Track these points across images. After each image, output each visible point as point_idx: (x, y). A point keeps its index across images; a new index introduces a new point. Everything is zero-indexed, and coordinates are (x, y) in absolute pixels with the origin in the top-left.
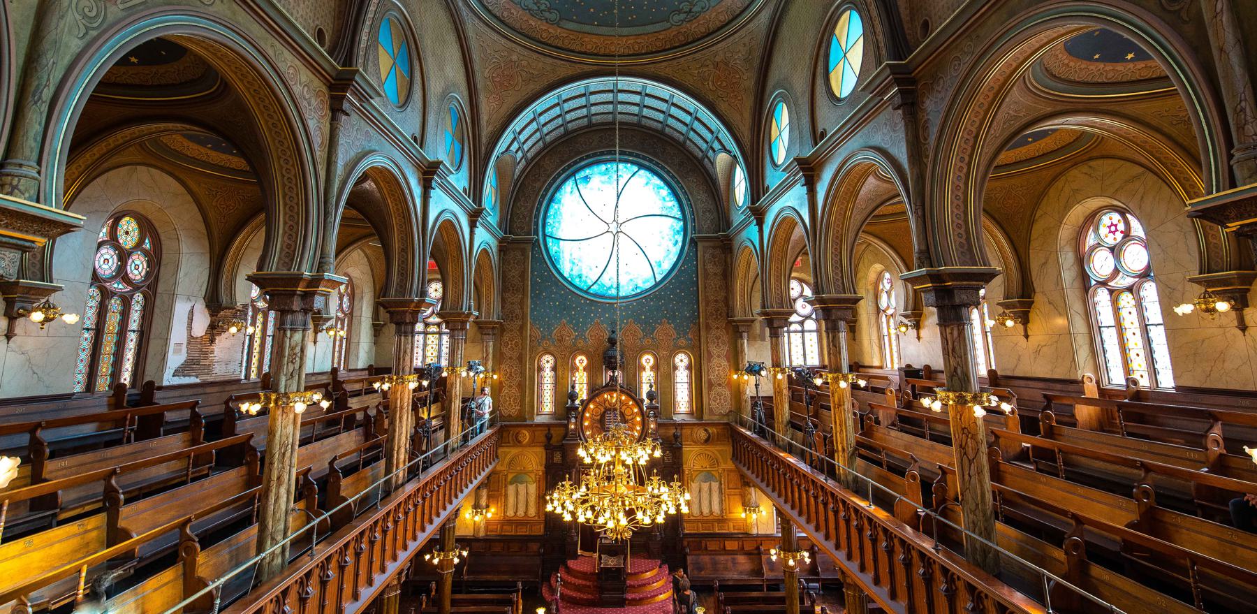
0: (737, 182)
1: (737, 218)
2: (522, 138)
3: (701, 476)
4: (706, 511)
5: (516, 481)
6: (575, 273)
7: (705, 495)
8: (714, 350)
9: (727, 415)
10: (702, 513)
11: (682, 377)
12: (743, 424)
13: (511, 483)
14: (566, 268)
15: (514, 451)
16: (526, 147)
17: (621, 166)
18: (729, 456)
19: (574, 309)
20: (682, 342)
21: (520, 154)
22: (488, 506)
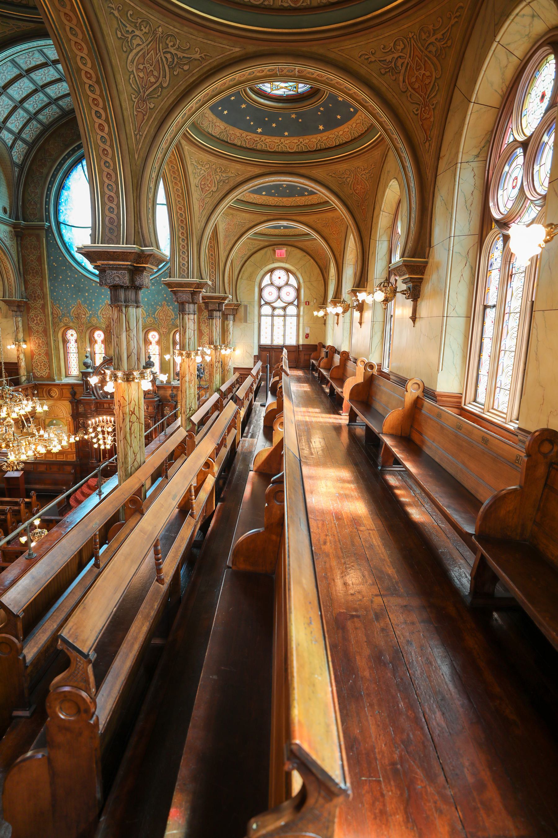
19: (88, 291)
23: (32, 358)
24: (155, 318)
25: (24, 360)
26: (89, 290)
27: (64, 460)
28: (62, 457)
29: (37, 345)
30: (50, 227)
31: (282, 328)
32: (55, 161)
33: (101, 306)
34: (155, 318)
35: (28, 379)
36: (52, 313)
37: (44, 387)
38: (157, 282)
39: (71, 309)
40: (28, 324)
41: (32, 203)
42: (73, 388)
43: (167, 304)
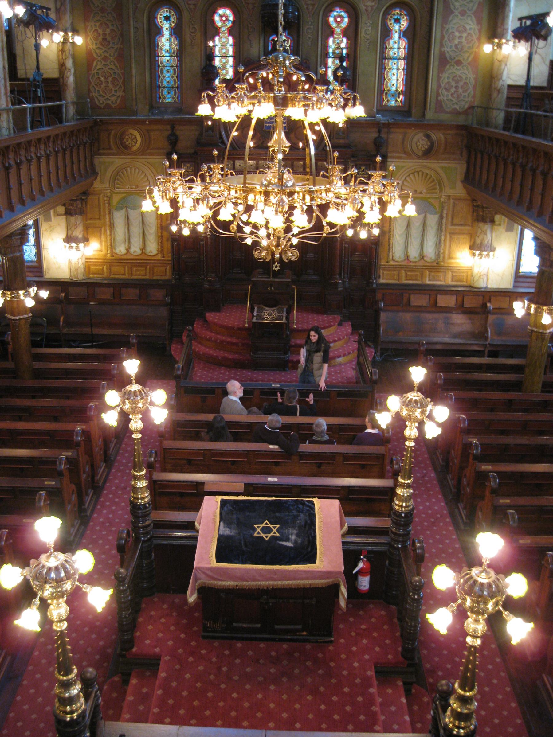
4: (414, 253)
9: (466, 112)
10: (407, 257)
11: (397, 46)
13: (119, 208)
15: (118, 161)
22: (86, 240)
23: (89, 66)
25: (72, 71)
27: (147, 277)
28: (143, 272)
29: (100, 39)
35: (81, 113)
42: (173, 128)
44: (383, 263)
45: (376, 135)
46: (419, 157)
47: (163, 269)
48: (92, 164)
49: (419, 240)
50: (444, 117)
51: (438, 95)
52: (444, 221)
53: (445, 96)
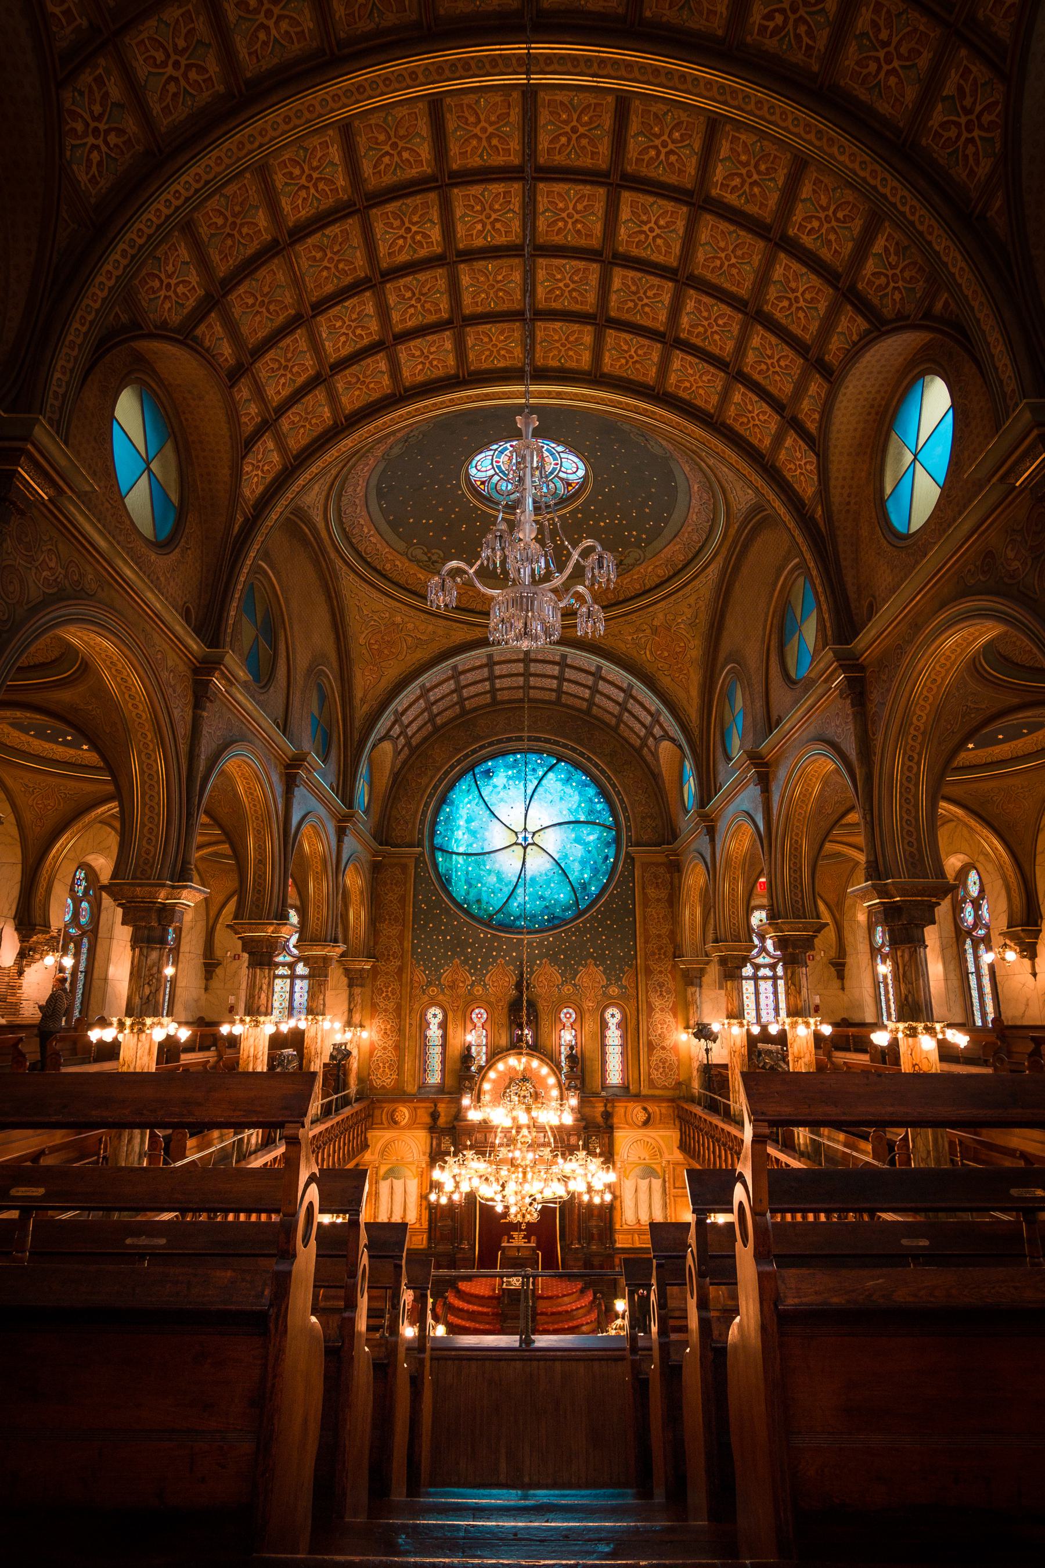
0: (686, 778)
1: (687, 822)
2: (405, 720)
3: (637, 1171)
5: (392, 1173)
6: (472, 897)
7: (643, 1197)
8: (657, 1003)
11: (614, 1036)
12: (692, 1100)
13: (385, 1178)
14: (459, 889)
16: (409, 732)
17: (533, 757)
18: (676, 1143)
19: (471, 945)
20: (614, 991)
21: (402, 740)
24: (575, 985)
26: (474, 943)
30: (422, 854)
31: (772, 997)
32: (439, 769)
33: (490, 967)
34: (575, 985)
36: (411, 980)
37: (384, 1105)
38: (578, 929)
39: (442, 974)
40: (372, 999)
41: (402, 822)
42: (436, 1106)
43: (595, 964)
44: (617, 1227)
45: (603, 1109)
46: (639, 1127)
47: (420, 1237)
48: (366, 1138)
49: (647, 1204)
50: (657, 1092)
51: (650, 1074)
52: (667, 1184)
53: (655, 1075)
